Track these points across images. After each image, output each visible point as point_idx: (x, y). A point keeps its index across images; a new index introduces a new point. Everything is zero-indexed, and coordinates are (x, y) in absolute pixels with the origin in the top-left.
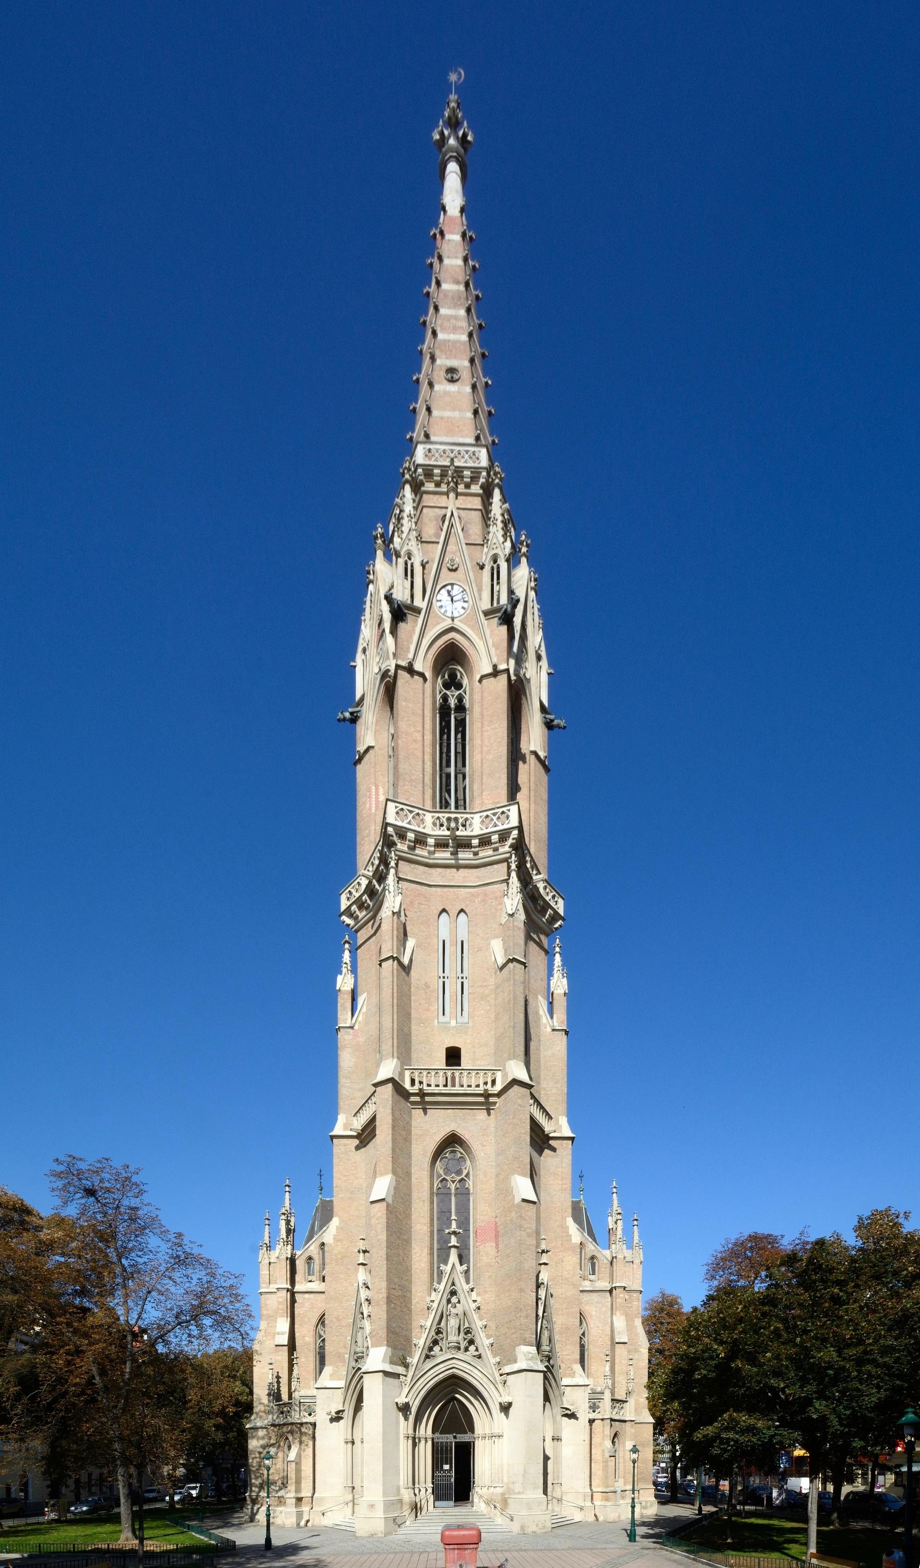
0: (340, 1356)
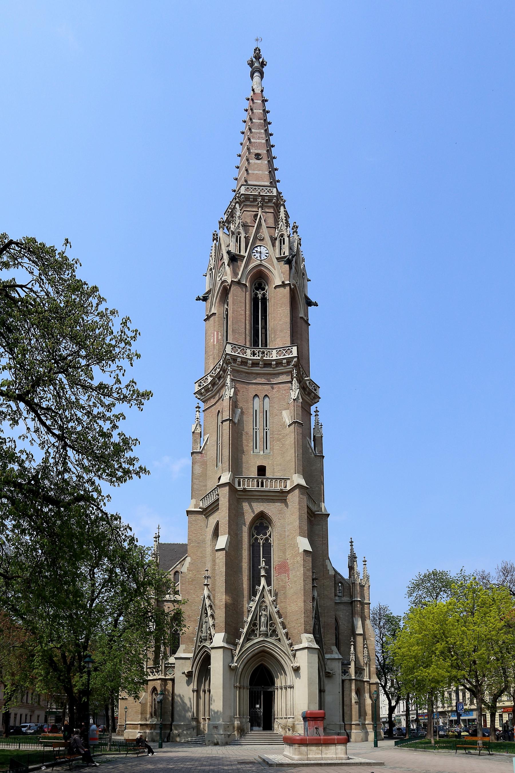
0: (190, 640)
